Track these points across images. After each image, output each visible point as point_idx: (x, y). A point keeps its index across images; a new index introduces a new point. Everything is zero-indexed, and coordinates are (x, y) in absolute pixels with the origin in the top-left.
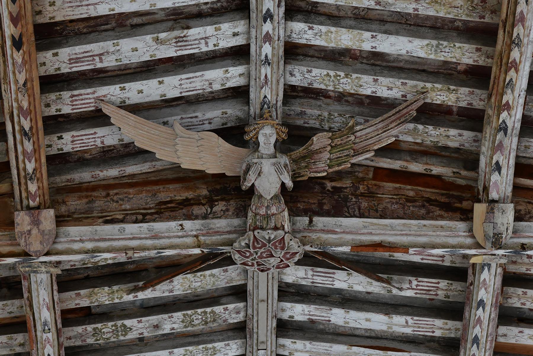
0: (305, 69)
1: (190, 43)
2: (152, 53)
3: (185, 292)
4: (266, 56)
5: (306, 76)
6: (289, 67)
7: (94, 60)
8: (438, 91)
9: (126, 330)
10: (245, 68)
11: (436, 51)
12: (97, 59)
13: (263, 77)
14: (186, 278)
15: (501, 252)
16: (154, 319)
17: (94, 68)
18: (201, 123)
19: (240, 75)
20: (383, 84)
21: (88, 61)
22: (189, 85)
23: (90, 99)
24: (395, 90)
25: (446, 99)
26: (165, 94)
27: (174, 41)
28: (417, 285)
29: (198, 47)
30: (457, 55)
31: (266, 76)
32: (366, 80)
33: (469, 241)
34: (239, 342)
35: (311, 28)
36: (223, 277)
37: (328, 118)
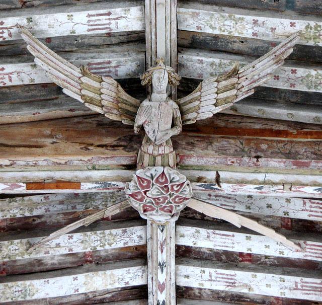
0: (130, 244)
1: (224, 280)
2: (255, 279)
3: (241, 16)
4: (162, 271)
5: (128, 239)
6: (142, 243)
7: (302, 286)
8: (18, 254)
10: (179, 242)
11: (26, 291)
12: (299, 287)
13: (165, 250)
14: (239, 33)
17: (303, 278)
18: (217, 198)
19: (183, 236)
20: (64, 248)
21: (307, 286)
22: (225, 241)
23: (309, 252)
24: (53, 244)
25: (10, 247)
26: (247, 239)
27: (236, 285)
28: (3, 33)
29: (217, 274)
30: (8, 291)
31: (162, 252)
32: (79, 249)
35: (127, 283)
36: (201, 22)
37: (107, 201)
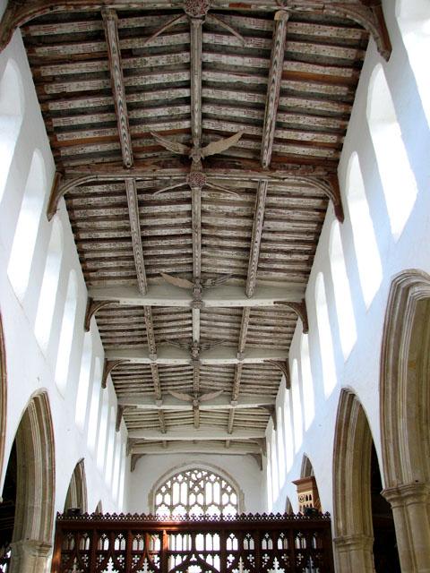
9: (146, 62)
15: (287, 8)
16: (156, 58)
33: (275, 3)
34: (188, 72)
